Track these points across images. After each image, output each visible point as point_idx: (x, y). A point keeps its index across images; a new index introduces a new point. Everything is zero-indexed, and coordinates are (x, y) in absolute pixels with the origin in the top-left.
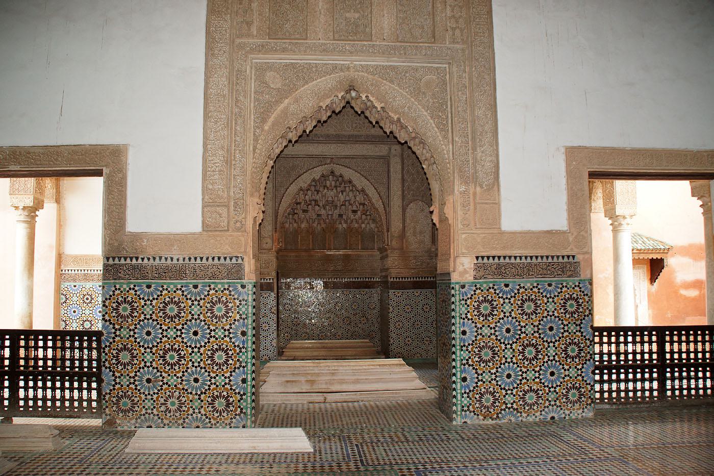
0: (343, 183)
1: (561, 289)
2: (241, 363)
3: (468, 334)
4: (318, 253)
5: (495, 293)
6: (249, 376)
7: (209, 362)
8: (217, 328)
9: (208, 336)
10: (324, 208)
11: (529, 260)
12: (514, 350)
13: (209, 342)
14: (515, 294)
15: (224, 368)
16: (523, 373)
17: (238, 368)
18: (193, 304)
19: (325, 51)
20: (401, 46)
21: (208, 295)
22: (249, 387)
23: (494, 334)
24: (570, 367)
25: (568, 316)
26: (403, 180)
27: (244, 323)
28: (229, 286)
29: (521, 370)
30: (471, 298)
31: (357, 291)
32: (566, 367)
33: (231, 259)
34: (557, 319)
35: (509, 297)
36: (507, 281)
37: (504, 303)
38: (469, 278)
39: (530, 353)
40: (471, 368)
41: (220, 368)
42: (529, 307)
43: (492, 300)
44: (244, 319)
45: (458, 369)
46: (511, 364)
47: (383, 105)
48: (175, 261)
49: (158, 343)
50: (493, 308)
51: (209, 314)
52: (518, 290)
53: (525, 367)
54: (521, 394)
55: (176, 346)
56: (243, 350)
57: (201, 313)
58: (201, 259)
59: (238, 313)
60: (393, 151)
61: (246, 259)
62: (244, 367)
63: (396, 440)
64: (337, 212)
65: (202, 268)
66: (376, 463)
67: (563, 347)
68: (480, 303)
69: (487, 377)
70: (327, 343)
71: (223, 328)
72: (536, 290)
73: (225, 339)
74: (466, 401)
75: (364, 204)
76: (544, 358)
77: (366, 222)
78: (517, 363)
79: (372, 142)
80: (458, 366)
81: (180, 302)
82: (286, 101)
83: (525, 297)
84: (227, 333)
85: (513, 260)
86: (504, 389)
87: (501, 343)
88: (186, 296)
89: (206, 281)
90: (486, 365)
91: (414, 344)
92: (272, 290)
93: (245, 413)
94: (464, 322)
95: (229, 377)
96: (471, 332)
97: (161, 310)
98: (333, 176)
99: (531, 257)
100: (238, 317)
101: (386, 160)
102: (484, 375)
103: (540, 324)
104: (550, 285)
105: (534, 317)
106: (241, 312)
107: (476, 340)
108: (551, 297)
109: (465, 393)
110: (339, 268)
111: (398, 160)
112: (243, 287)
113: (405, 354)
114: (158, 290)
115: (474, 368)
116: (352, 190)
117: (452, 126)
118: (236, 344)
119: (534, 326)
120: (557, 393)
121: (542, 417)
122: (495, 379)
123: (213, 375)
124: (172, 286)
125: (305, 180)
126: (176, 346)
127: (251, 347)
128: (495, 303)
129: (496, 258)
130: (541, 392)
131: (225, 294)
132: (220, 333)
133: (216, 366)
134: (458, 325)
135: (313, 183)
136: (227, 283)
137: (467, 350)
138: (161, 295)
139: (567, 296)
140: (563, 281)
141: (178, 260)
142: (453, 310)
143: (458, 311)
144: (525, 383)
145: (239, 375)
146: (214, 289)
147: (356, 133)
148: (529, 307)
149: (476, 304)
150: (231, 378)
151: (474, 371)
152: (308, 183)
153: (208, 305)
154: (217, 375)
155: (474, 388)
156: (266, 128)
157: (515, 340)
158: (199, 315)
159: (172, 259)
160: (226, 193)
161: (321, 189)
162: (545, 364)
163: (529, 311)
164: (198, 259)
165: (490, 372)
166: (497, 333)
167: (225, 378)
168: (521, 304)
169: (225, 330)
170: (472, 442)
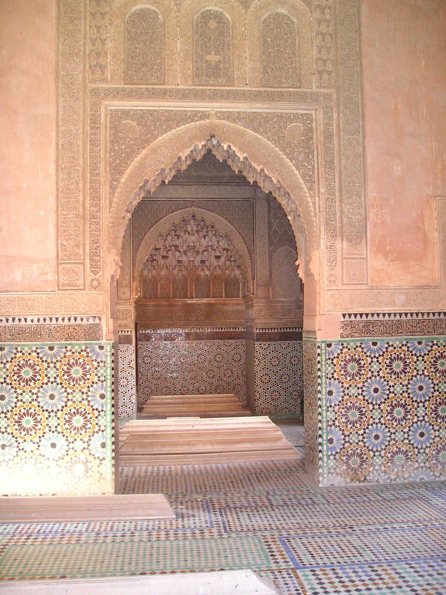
1: (432, 347)
4: (179, 302)
5: (362, 352)
11: (398, 317)
12: (382, 411)
14: (384, 353)
16: (391, 433)
18: (49, 367)
19: (184, 95)
20: (265, 92)
24: (440, 428)
25: (438, 375)
27: (102, 385)
28: (87, 348)
29: (389, 431)
30: (338, 357)
31: (221, 342)
32: (436, 428)
34: (427, 378)
35: (377, 355)
36: (375, 339)
37: (372, 361)
38: (335, 337)
39: (399, 413)
40: (338, 429)
42: (398, 366)
43: (360, 359)
44: (102, 382)
45: (325, 431)
46: (379, 425)
47: (245, 155)
48: (29, 322)
49: (13, 408)
50: (361, 367)
51: (66, 377)
52: (387, 348)
53: (393, 428)
54: (389, 455)
55: (32, 411)
57: (58, 376)
58: (57, 319)
59: (96, 375)
61: (104, 319)
62: (103, 431)
63: (260, 504)
65: (58, 329)
66: (239, 529)
67: (433, 407)
68: (347, 362)
69: (354, 438)
70: (190, 398)
72: (405, 348)
74: (332, 463)
75: (228, 250)
76: (413, 418)
78: (385, 424)
80: (325, 427)
81: (35, 365)
82: (144, 151)
83: (393, 355)
85: (381, 318)
86: (372, 450)
87: (368, 403)
88: (41, 358)
89: (63, 342)
91: (282, 399)
92: (130, 343)
93: (104, 478)
94: (330, 383)
97: (15, 373)
98: (195, 220)
99: (401, 315)
100: (96, 379)
102: (351, 436)
103: (409, 383)
104: (420, 343)
105: (402, 376)
107: (343, 400)
108: (420, 356)
109: (332, 455)
112: (101, 348)
113: (272, 409)
114: (12, 352)
119: (403, 386)
120: (427, 454)
121: (411, 479)
122: (362, 441)
124: (26, 348)
126: (32, 411)
128: (362, 362)
129: (364, 315)
130: (410, 454)
131: (83, 356)
134: (324, 385)
135: (173, 228)
136: (85, 344)
137: (334, 411)
138: (15, 358)
139: (438, 354)
140: (434, 338)
141: (32, 321)
142: (319, 370)
143: (324, 371)
144: (394, 445)
146: (71, 351)
148: (398, 366)
149: (342, 364)
151: (341, 432)
153: (65, 368)
155: (341, 449)
156: (123, 180)
157: (383, 400)
158: (55, 378)
159: (26, 320)
160: (82, 250)
161: (182, 234)
162: (415, 425)
163: (398, 370)
164: (54, 320)
165: (357, 433)
166: (364, 393)
168: (390, 362)
169: (83, 393)
170: (338, 506)
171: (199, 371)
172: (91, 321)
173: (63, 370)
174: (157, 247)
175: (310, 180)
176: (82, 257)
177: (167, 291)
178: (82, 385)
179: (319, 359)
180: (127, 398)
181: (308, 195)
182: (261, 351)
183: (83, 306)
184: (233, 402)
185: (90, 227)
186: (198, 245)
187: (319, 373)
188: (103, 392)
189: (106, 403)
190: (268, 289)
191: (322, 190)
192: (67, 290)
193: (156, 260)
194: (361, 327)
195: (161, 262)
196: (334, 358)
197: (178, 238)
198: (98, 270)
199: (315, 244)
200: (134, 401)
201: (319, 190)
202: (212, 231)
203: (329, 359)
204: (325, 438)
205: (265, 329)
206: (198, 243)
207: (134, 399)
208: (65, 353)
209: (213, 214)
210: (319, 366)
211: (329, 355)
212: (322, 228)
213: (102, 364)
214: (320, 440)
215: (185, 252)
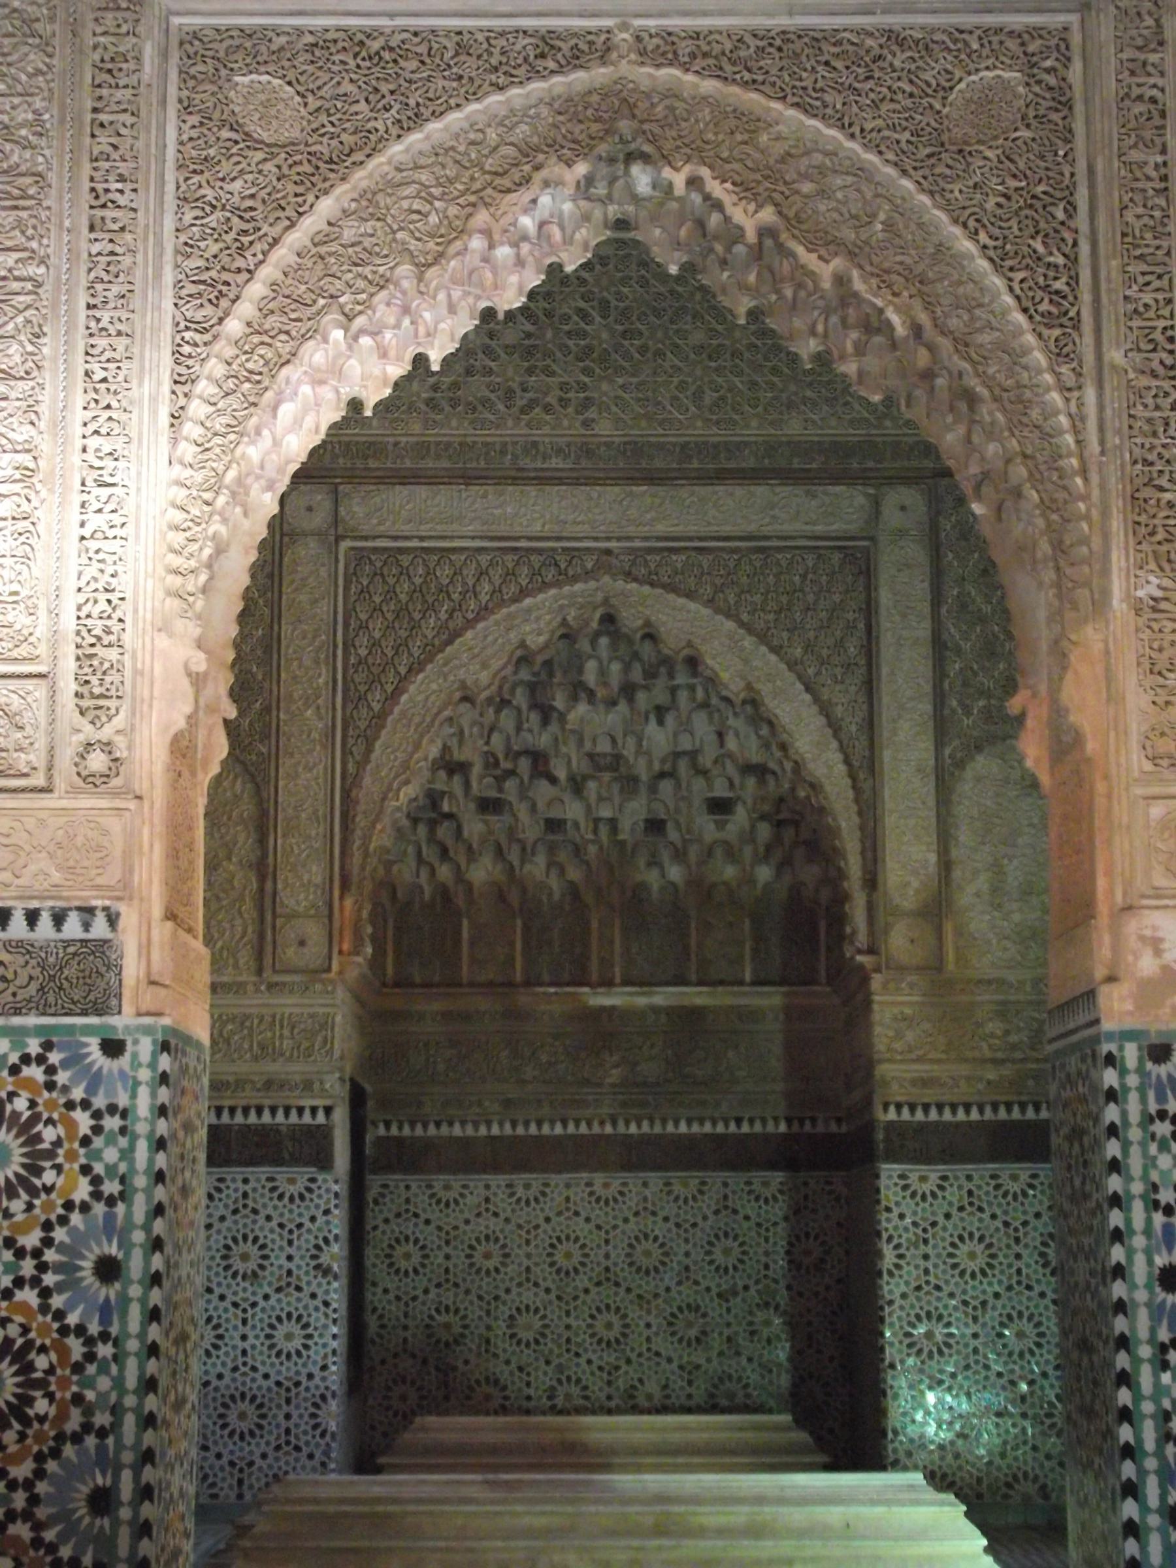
0: (661, 672)
2: (88, 1411)
4: (550, 1002)
6: (127, 1476)
22: (124, 1534)
26: (939, 646)
27: (110, 1218)
28: (48, 1046)
31: (736, 1180)
33: (59, 919)
45: (1151, 1464)
47: (768, 215)
56: (105, 1350)
59: (86, 1170)
60: (892, 517)
61: (129, 918)
75: (760, 771)
79: (787, 476)
80: (1150, 1445)
82: (327, 206)
84: (28, 1267)
92: (324, 1162)
95: (28, 1485)
100: (82, 1191)
101: (858, 561)
106: (99, 1168)
111: (916, 552)
112: (113, 1047)
116: (705, 705)
117: (1097, 300)
118: (72, 1319)
125: (481, 654)
127: (142, 1335)
131: (29, 1083)
134: (1139, 1241)
136: (39, 1030)
142: (1115, 1166)
145: (74, 1472)
147: (716, 435)
150: (41, 1488)
152: (496, 664)
161: (559, 703)
171: (634, 1313)
172: (73, 928)
174: (458, 756)
175: (1056, 315)
176: (42, 650)
179: (1112, 1113)
181: (1048, 378)
182: (908, 1206)
183: (41, 862)
186: (629, 751)
187: (1114, 1183)
188: (113, 1250)
189: (124, 1300)
191: (1115, 356)
193: (450, 816)
195: (474, 827)
197: (545, 722)
198: (112, 704)
199: (1083, 594)
200: (333, 1426)
201: (1099, 357)
204: (1153, 1501)
206: (631, 741)
209: (693, 606)
210: (1113, 1149)
212: (1116, 524)
213: (112, 1123)
214: (1129, 1509)
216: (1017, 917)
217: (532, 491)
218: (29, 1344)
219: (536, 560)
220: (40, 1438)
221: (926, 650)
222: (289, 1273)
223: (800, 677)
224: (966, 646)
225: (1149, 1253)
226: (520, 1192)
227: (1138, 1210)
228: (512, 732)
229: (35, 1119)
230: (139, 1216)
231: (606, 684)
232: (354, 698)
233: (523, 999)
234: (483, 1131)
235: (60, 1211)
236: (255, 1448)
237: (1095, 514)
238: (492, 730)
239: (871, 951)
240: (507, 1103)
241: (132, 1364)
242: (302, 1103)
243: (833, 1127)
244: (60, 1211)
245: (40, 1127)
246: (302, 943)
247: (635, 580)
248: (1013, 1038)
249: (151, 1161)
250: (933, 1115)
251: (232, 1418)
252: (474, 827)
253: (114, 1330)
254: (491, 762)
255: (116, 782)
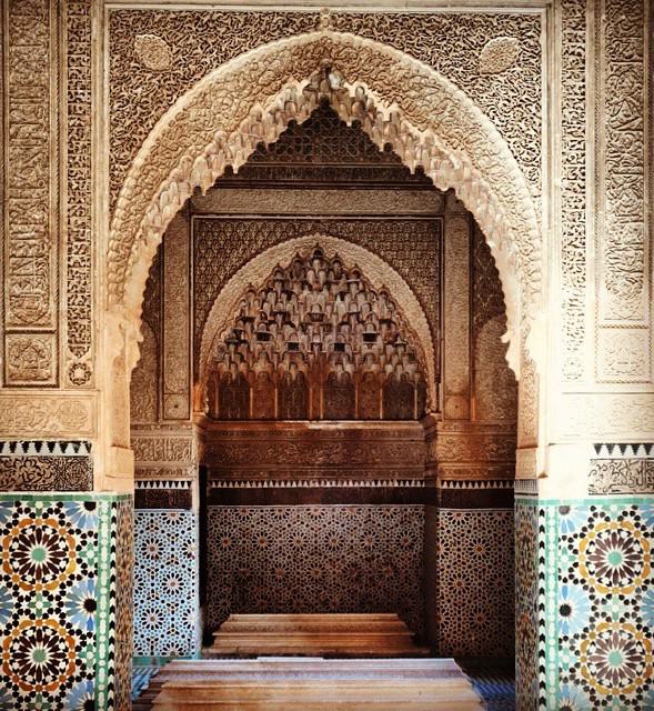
0: (342, 277)
2: (84, 667)
3: (573, 613)
4: (291, 427)
5: (637, 525)
6: (101, 695)
7: (16, 666)
8: (33, 594)
9: (15, 611)
10: (304, 331)
13: (16, 624)
15: (49, 678)
17: (79, 679)
21: (16, 523)
23: (634, 615)
27: (91, 582)
28: (60, 505)
33: (64, 446)
40: (581, 687)
41: (39, 679)
43: (630, 541)
51: (16, 565)
56: (90, 641)
59: (79, 561)
62: (90, 677)
64: (332, 337)
71: (45, 593)
73: (51, 617)
75: (389, 322)
77: (395, 360)
84: (54, 604)
90: (616, 681)
94: (565, 588)
96: (582, 609)
98: (322, 260)
100: (78, 570)
106: (85, 560)
110: (337, 459)
115: (586, 689)
116: (363, 291)
118: (75, 628)
123: (23, 693)
125: (258, 270)
127: (106, 634)
132: (40, 604)
133: (31, 674)
135: (279, 277)
136: (56, 498)
146: (27, 510)
152: (266, 275)
153: (16, 546)
154: (33, 694)
160: (53, 305)
161: (296, 290)
167: (51, 699)
169: (51, 598)
173: (11, 550)
176: (53, 320)
177: (268, 403)
178: (50, 582)
180: (178, 617)
184: (396, 629)
185: (69, 259)
188: (93, 597)
189: (98, 619)
190: (469, 402)
192: (22, 386)
193: (245, 342)
194: (634, 473)
195: (256, 346)
196: (576, 536)
197: (289, 299)
198: (86, 346)
202: (357, 283)
203: (564, 538)
205: (461, 483)
206: (329, 308)
207: (195, 618)
208: (16, 516)
211: (564, 530)
213: (90, 540)
215: (304, 327)
216: (505, 397)
217: (283, 192)
218: (56, 639)
219: (284, 225)
220: (62, 679)
221: (467, 270)
222: (173, 556)
223: (407, 283)
224: (485, 269)
225: (555, 598)
226: (277, 513)
227: (552, 580)
228: (273, 303)
229: (56, 538)
230: (104, 583)
231: (317, 282)
232: (199, 291)
233: (278, 426)
234: (260, 486)
235: (68, 579)
236: (160, 632)
237: (545, 258)
238: (264, 301)
239: (438, 411)
240: (271, 473)
241: (102, 647)
242: (177, 480)
243: (419, 485)
244: (68, 579)
245: (58, 542)
246: (176, 406)
247: (331, 235)
248: (501, 451)
249: (109, 557)
250: (464, 487)
251: (148, 619)
252: (256, 346)
253: (94, 632)
254: (264, 317)
255: (88, 383)
